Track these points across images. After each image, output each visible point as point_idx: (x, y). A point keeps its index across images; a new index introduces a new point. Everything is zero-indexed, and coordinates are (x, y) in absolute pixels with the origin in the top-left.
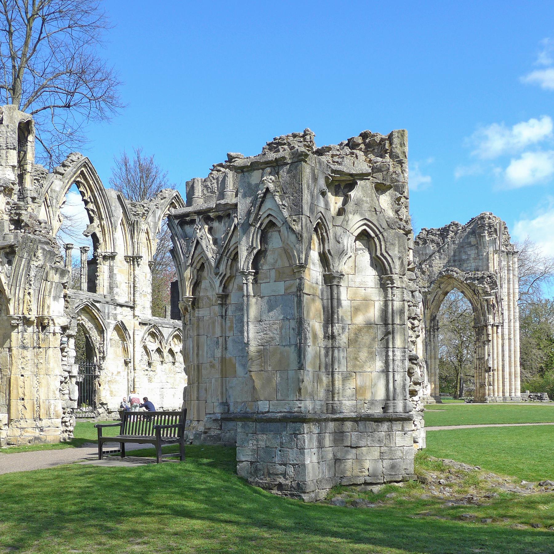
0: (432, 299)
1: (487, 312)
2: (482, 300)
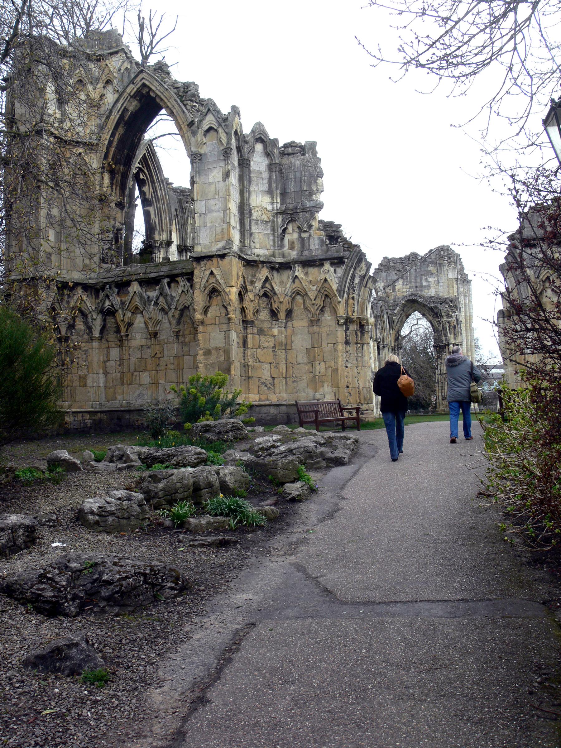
0: (397, 321)
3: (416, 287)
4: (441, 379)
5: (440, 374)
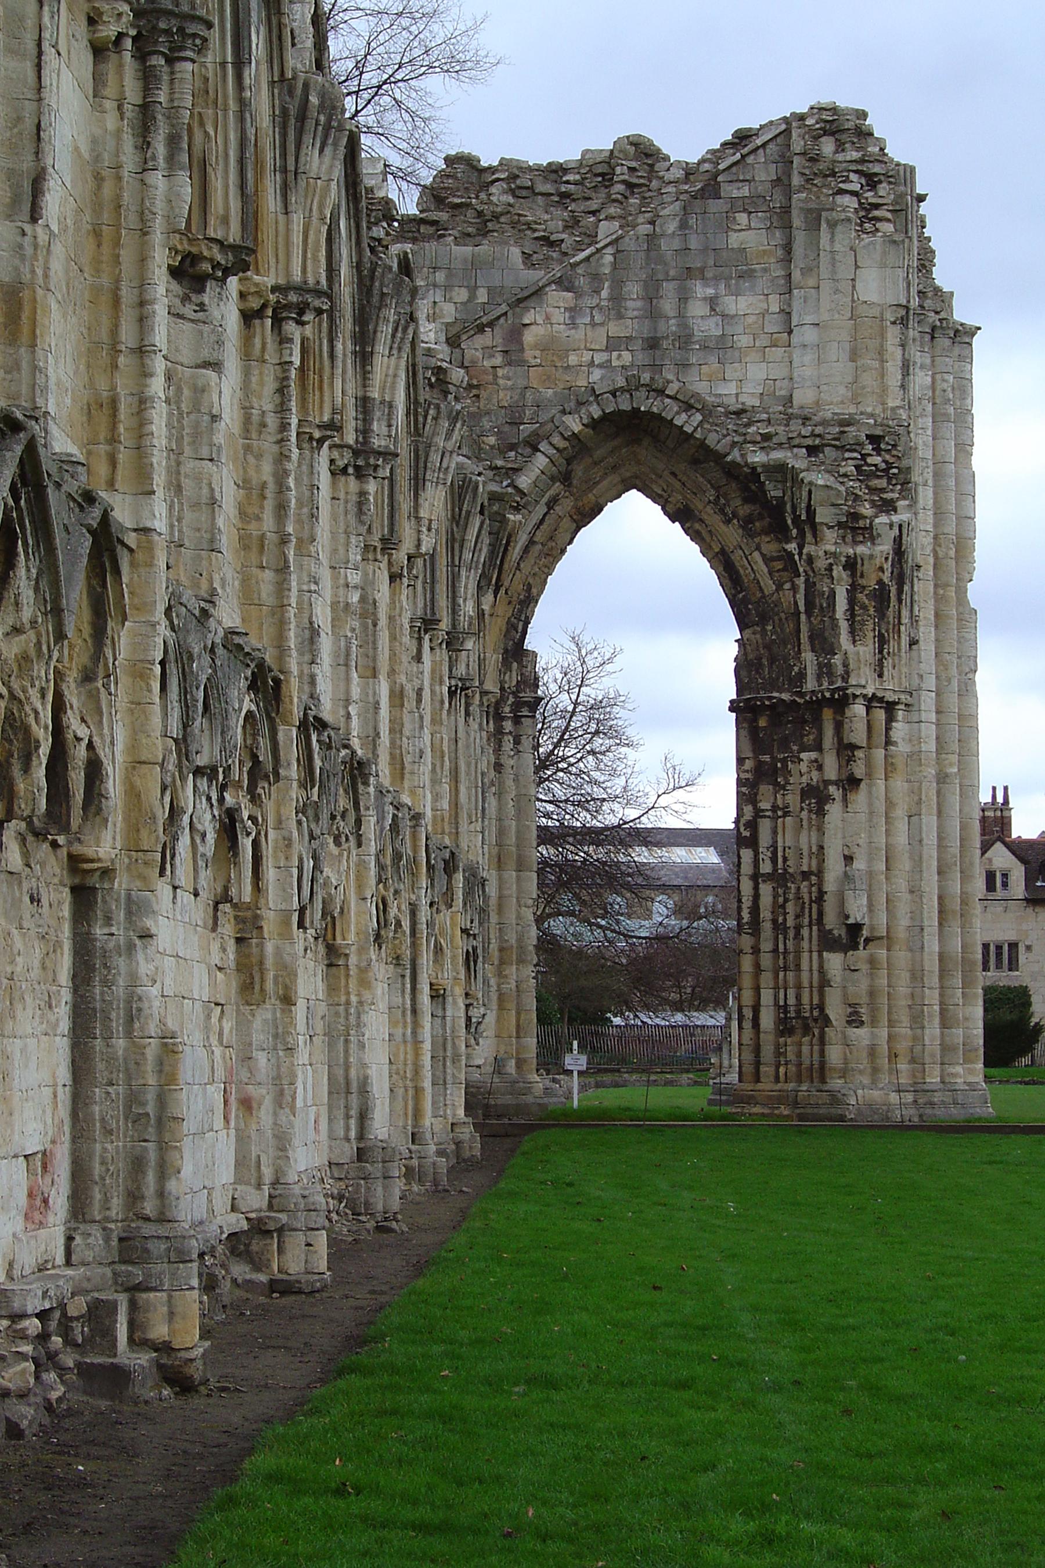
0: (522, 539)
1: (844, 626)
2: (821, 564)
3: (653, 344)
4: (779, 908)
5: (770, 877)
